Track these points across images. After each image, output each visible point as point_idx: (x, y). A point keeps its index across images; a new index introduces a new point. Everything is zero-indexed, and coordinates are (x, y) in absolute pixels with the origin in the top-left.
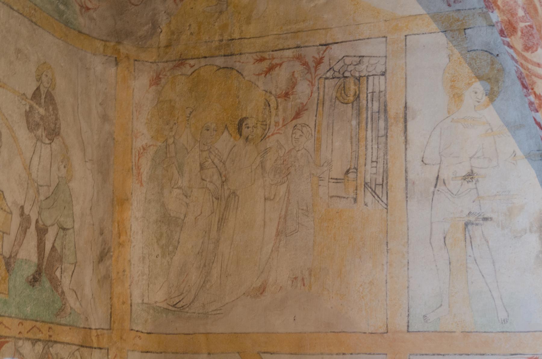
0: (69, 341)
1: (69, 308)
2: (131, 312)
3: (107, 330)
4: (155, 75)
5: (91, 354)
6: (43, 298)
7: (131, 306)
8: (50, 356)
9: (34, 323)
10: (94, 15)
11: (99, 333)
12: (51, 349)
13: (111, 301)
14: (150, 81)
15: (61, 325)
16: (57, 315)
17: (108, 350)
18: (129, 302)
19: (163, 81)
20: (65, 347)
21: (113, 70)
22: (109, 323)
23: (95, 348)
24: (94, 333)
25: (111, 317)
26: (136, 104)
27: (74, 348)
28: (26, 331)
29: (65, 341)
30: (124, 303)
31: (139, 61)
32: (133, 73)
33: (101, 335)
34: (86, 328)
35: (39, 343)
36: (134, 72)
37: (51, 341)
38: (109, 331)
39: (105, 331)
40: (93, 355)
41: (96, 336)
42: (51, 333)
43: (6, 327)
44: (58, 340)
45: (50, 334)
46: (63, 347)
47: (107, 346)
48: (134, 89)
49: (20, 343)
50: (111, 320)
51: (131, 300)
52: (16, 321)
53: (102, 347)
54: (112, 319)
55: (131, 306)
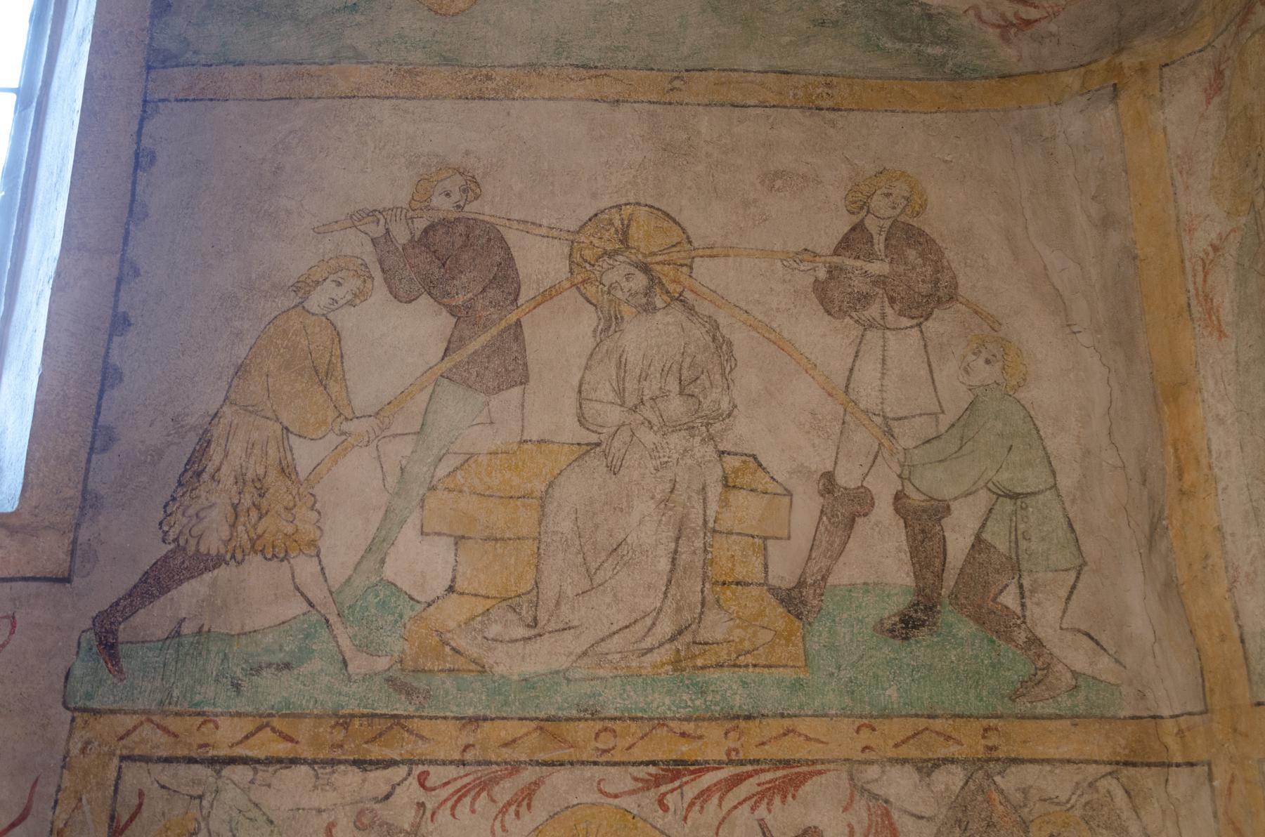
0: (1074, 756)
1: (1069, 675)
2: (1246, 658)
3: (1201, 713)
4: (1212, 71)
5: (1167, 781)
6: (952, 662)
7: (1242, 641)
8: (995, 795)
9: (922, 723)
10: (1053, 28)
11: (1184, 727)
12: (998, 779)
13: (1194, 640)
14: (1206, 90)
15: (1036, 718)
16: (1014, 697)
17: (1209, 765)
18: (1236, 633)
19: (1227, 73)
20: (1057, 771)
21: (1108, 113)
22: (1201, 696)
23: (1178, 765)
24: (1169, 726)
25: (1203, 681)
26: (1178, 157)
27: (1092, 770)
28: (891, 743)
29: (1057, 757)
30: (1223, 638)
31: (1173, 63)
32: (1158, 94)
33: (1189, 729)
34: (1141, 718)
35: (953, 768)
36: (1161, 91)
37: (998, 760)
38: (1204, 716)
39: (1197, 719)
40: (1170, 782)
41: (1177, 734)
42: (993, 740)
43: (808, 739)
44: (1025, 753)
45: (990, 745)
46: (1051, 771)
47: (1205, 757)
48: (1165, 129)
49: (873, 772)
50: (1204, 687)
51: (1240, 626)
52: (847, 725)
53: (1194, 760)
54: (1207, 685)
55: (1242, 641)
